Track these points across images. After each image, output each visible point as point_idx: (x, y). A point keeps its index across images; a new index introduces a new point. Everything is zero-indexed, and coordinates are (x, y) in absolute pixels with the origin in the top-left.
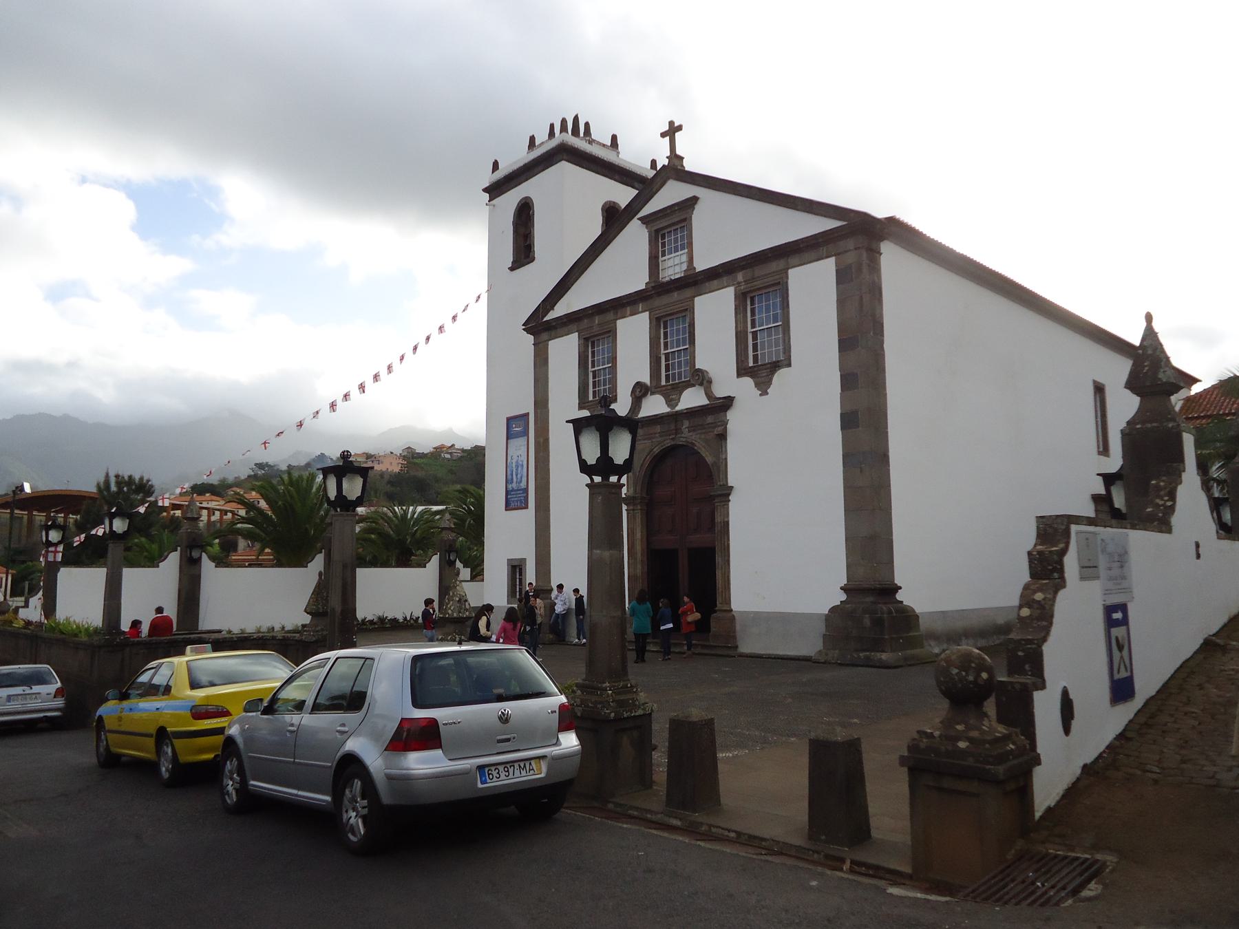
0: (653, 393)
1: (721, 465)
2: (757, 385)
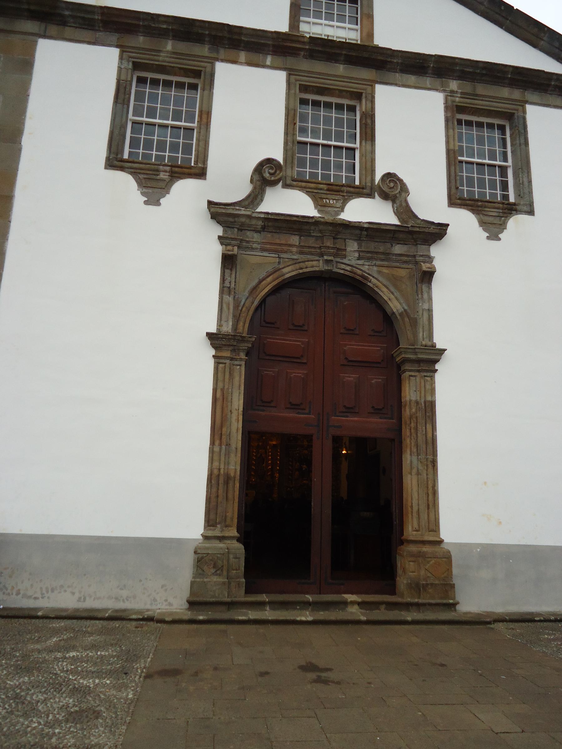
0: (286, 186)
1: (420, 318)
2: (482, 224)
